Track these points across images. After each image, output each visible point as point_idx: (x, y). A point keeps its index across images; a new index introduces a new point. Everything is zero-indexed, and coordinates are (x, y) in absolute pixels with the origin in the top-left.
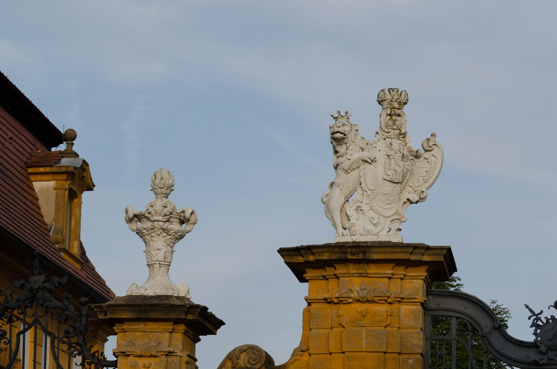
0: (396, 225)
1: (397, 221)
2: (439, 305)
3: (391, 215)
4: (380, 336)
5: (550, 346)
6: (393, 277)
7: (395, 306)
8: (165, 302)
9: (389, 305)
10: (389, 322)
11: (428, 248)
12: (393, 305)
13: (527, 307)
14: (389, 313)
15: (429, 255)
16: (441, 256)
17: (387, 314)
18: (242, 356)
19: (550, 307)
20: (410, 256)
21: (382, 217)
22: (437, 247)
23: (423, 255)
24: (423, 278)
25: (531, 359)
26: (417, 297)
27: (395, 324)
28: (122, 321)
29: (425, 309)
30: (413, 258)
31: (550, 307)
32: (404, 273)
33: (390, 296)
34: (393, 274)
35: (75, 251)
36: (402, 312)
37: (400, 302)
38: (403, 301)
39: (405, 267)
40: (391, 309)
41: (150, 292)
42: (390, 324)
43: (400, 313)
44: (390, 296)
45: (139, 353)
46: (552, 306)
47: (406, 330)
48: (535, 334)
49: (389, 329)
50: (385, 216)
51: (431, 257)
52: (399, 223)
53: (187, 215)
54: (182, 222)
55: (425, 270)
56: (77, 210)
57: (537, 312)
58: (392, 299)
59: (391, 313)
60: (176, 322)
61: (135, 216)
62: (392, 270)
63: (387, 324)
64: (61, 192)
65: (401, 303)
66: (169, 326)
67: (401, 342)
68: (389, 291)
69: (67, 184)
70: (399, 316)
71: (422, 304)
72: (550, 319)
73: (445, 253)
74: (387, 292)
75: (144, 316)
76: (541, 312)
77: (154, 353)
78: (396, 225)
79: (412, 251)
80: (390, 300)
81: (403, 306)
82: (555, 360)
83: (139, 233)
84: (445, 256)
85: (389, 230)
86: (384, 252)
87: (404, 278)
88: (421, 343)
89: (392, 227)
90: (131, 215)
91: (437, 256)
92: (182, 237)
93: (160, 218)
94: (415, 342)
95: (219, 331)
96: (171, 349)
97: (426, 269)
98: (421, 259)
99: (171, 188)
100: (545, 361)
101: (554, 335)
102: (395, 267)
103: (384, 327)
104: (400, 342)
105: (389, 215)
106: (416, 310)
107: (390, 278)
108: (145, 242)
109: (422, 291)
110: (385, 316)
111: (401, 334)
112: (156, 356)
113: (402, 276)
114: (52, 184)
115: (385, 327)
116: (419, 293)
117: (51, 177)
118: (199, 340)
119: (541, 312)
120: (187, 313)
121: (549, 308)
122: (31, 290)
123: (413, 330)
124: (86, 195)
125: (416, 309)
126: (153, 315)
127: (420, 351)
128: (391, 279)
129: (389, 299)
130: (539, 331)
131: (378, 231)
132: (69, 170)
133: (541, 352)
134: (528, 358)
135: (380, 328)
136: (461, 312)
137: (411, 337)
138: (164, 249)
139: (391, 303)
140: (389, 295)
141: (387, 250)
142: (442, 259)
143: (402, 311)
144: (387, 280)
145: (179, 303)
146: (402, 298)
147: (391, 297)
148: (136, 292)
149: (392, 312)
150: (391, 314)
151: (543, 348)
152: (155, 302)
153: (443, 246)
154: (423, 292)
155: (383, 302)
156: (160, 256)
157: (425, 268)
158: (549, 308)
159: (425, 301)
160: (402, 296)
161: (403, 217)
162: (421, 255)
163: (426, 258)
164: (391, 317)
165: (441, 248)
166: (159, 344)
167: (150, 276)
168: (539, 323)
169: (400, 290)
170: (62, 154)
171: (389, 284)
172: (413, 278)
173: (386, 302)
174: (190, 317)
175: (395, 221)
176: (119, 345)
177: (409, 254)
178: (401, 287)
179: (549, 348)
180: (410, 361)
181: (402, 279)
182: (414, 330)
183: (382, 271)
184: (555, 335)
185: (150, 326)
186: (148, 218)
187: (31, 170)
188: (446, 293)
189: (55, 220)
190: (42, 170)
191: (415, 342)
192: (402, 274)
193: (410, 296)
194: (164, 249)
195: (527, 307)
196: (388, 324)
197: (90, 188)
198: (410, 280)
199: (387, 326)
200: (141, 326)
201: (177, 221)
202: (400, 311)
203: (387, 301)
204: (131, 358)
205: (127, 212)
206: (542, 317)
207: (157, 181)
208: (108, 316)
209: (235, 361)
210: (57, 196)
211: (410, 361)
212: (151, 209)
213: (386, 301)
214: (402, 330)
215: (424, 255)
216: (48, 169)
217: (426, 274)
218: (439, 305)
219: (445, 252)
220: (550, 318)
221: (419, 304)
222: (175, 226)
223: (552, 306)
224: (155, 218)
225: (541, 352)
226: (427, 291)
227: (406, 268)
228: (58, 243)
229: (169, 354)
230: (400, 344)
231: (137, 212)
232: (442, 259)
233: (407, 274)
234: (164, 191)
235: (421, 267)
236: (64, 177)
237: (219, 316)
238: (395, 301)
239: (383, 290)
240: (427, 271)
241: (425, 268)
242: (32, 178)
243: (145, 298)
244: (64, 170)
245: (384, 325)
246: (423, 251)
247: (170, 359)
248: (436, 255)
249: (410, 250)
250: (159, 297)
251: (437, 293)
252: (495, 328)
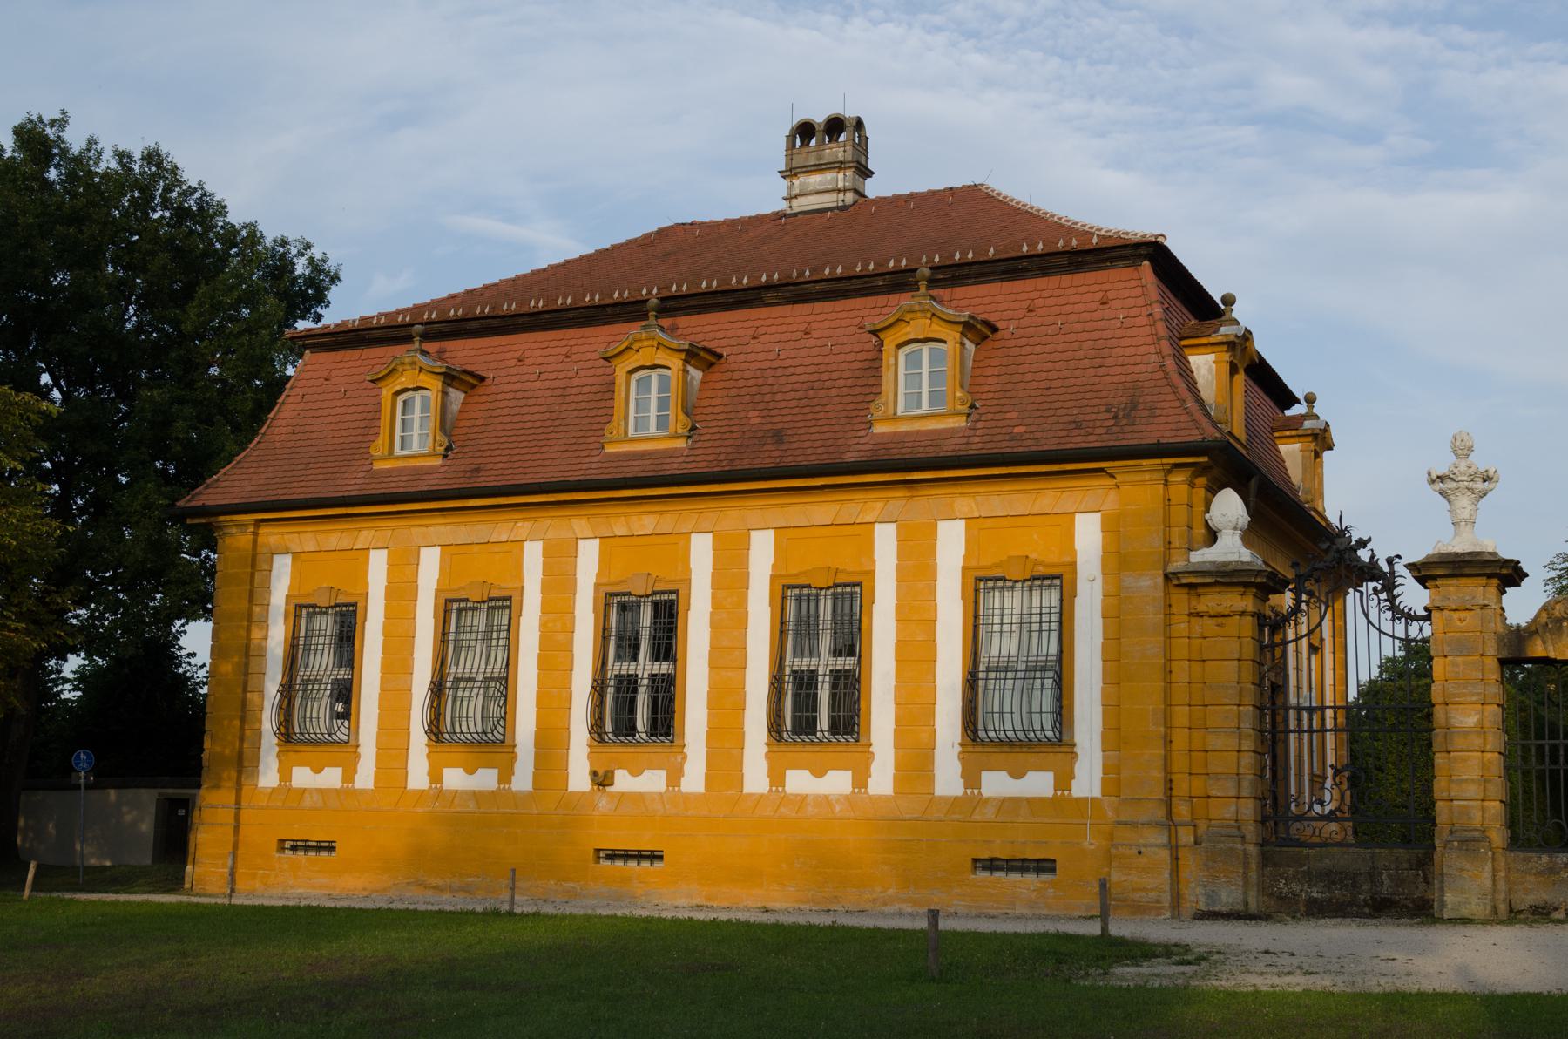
8: (1478, 558)
18: (1558, 607)
28: (1435, 578)
35: (1320, 509)
41: (1458, 549)
45: (1454, 607)
53: (1491, 474)
54: (1485, 481)
56: (1319, 470)
60: (1489, 576)
61: (1438, 477)
64: (1307, 454)
66: (1483, 581)
69: (1312, 446)
75: (1457, 572)
77: (1469, 606)
83: (1443, 493)
90: (1434, 476)
92: (1485, 495)
93: (1465, 478)
95: (1523, 583)
96: (1486, 603)
99: (1471, 449)
108: (1449, 502)
112: (1471, 610)
114: (1297, 446)
117: (1297, 439)
118: (1505, 592)
120: (1501, 568)
122: (1338, 551)
124: (1326, 454)
126: (1467, 571)
132: (1315, 432)
138: (1469, 508)
145: (1492, 558)
148: (1444, 550)
152: (1468, 558)
156: (1466, 515)
166: (1474, 598)
167: (1456, 533)
170: (1303, 417)
174: (1504, 571)
176: (1432, 600)
185: (1464, 581)
186: (1452, 479)
187: (1276, 434)
189: (1303, 480)
190: (1288, 433)
194: (1469, 508)
197: (1330, 448)
200: (1455, 581)
201: (1480, 480)
204: (1445, 612)
205: (1429, 474)
207: (1458, 443)
208: (1423, 573)
209: (1551, 611)
210: (1303, 457)
212: (1455, 470)
216: (1294, 433)
222: (1479, 485)
224: (1460, 478)
228: (1308, 502)
229: (1484, 607)
231: (1440, 474)
234: (1465, 452)
236: (1310, 439)
237: (1525, 570)
242: (1278, 441)
243: (1457, 555)
244: (1309, 432)
247: (1485, 611)
250: (1470, 553)
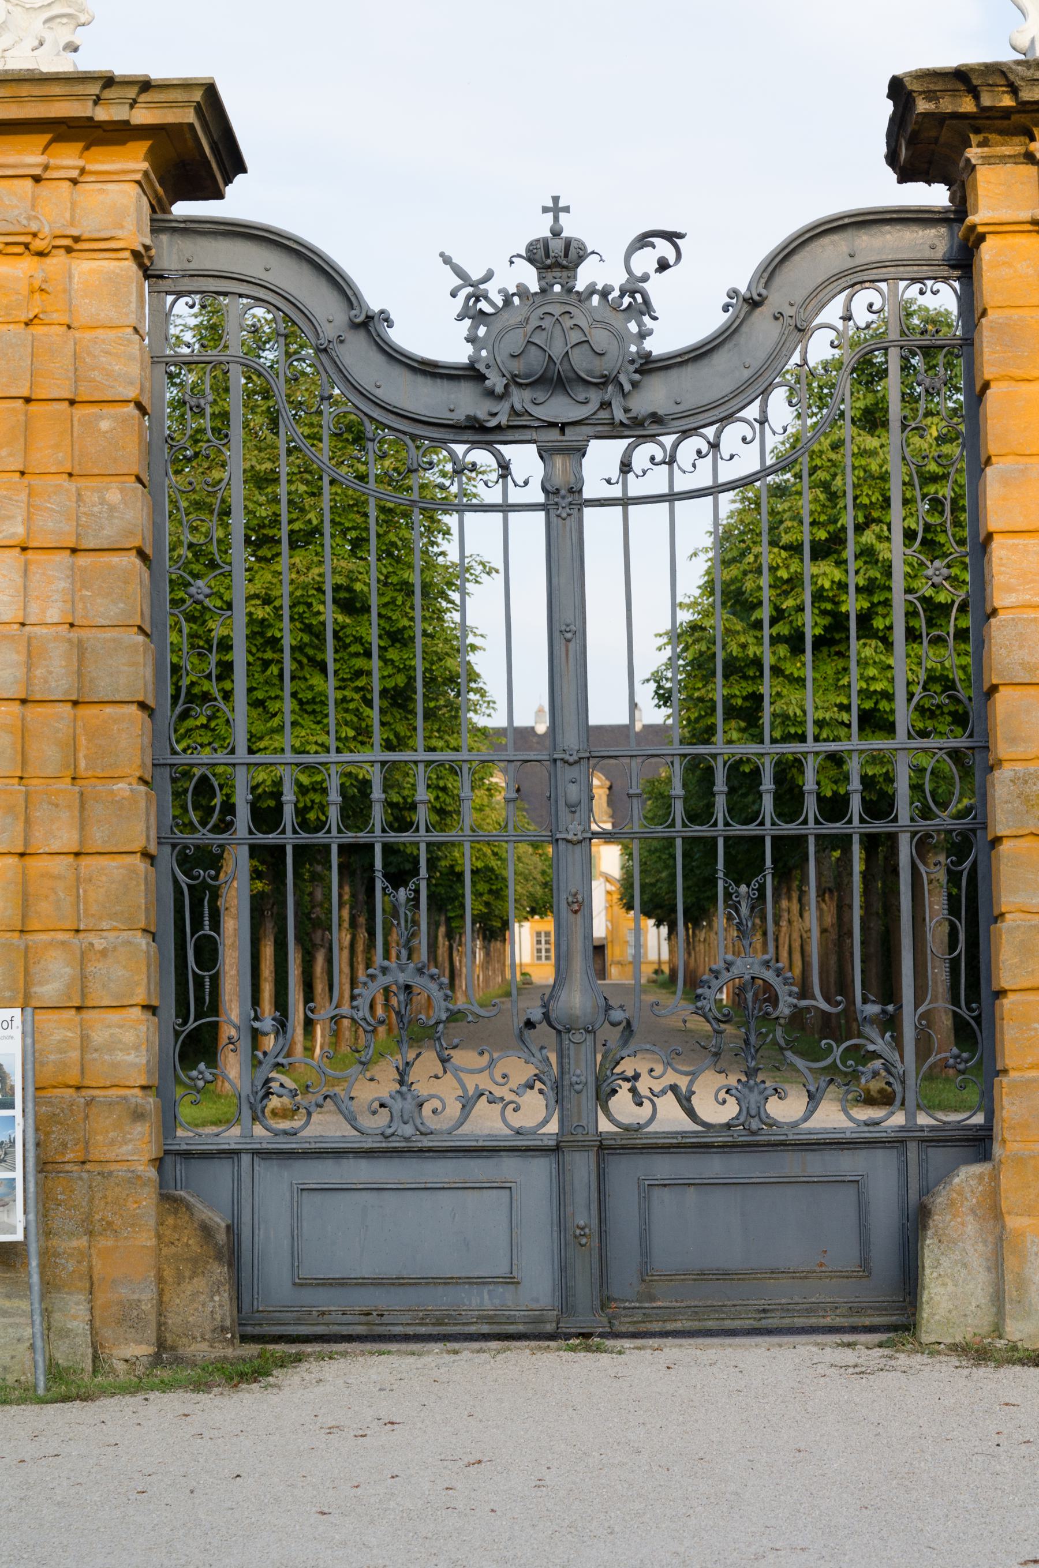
0: (64, 34)
1: (64, 20)
2: (189, 261)
3: (45, 3)
4: (11, 350)
5: (516, 376)
6: (47, 175)
7: (58, 261)
9: (36, 258)
10: (36, 311)
11: (146, 85)
12: (47, 260)
13: (447, 260)
14: (37, 284)
15: (151, 105)
16: (186, 110)
17: (31, 284)
19: (514, 259)
20: (93, 110)
21: (19, 9)
22: (175, 82)
23: (132, 106)
24: (138, 177)
25: (459, 416)
26: (119, 233)
27: (55, 315)
29: (149, 272)
30: (102, 114)
31: (514, 259)
32: (81, 163)
33: (39, 231)
34: (46, 167)
36: (76, 280)
37: (69, 250)
38: (78, 246)
39: (80, 145)
40: (43, 270)
42: (41, 316)
43: (70, 282)
44: (39, 231)
46: (519, 256)
47: (88, 335)
48: (471, 339)
49: (37, 330)
50: (28, 6)
51: (156, 111)
52: (72, 27)
55: (142, 155)
57: (476, 275)
58: (46, 242)
59: (43, 281)
62: (43, 154)
63: (31, 316)
65: (74, 254)
67: (76, 370)
68: (36, 218)
70: (67, 291)
71: (136, 255)
72: (513, 295)
73: (198, 99)
74: (29, 218)
76: (489, 276)
78: (64, 34)
79: (97, 92)
80: (38, 245)
81: (79, 261)
82: (532, 416)
84: (198, 109)
85: (36, 43)
86: (16, 99)
87: (81, 179)
88: (134, 370)
89: (48, 36)
91: (175, 110)
94: (117, 368)
97: (145, 149)
98: (125, 118)
100: (503, 419)
101: (528, 342)
102: (54, 145)
103: (23, 325)
104: (71, 368)
105: (40, 4)
106: (118, 274)
107: (37, 179)
109: (135, 215)
110: (25, 291)
111: (75, 344)
113: (74, 174)
115: (26, 324)
116: (125, 224)
119: (489, 276)
121: (512, 262)
123: (112, 334)
125: (118, 271)
127: (132, 393)
128: (43, 182)
129: (37, 241)
130: (482, 331)
131: (5, 47)
133: (490, 393)
134: (452, 411)
135: (11, 327)
136: (253, 280)
137: (106, 353)
139: (41, 254)
140: (34, 227)
141: (25, 90)
142: (189, 117)
143: (76, 275)
144: (29, 183)
146: (77, 239)
147: (41, 236)
149: (45, 281)
150: (43, 287)
151: (496, 382)
153: (191, 79)
154: (139, 220)
155: (20, 249)
157: (142, 147)
158: (512, 262)
159: (147, 248)
160: (75, 232)
161: (82, 11)
162: (127, 107)
163: (141, 116)
164: (45, 296)
165: (186, 85)
168: (483, 305)
169: (68, 215)
171: (34, 198)
172: (107, 178)
173: (27, 252)
175: (59, 20)
177: (91, 103)
178: (73, 204)
179: (514, 381)
180: (105, 425)
181: (74, 182)
182: (115, 331)
183: (12, 159)
184: (528, 342)
188: (209, 226)
191: (117, 368)
192: (74, 168)
193: (99, 231)
195: (447, 260)
196: (36, 316)
198: (99, 186)
199: (31, 320)
202: (70, 277)
203: (31, 247)
206: (492, 289)
211: (105, 425)
213: (27, 246)
214: (77, 334)
215: (137, 105)
217: (145, 166)
218: (189, 261)
219: (198, 96)
220: (515, 290)
221: (127, 254)
223: (519, 256)
225: (490, 393)
226: (152, 220)
227: (87, 148)
230: (71, 375)
232: (189, 117)
233: (90, 167)
235: (131, 145)
238: (54, 247)
239: (16, 212)
240: (152, 155)
241: (142, 147)
245: (24, 318)
246: (132, 93)
248: (172, 104)
249: (95, 89)
251: (182, 225)
252: (355, 326)
